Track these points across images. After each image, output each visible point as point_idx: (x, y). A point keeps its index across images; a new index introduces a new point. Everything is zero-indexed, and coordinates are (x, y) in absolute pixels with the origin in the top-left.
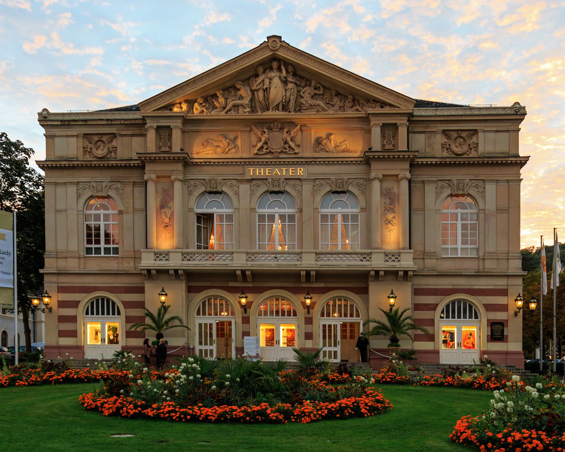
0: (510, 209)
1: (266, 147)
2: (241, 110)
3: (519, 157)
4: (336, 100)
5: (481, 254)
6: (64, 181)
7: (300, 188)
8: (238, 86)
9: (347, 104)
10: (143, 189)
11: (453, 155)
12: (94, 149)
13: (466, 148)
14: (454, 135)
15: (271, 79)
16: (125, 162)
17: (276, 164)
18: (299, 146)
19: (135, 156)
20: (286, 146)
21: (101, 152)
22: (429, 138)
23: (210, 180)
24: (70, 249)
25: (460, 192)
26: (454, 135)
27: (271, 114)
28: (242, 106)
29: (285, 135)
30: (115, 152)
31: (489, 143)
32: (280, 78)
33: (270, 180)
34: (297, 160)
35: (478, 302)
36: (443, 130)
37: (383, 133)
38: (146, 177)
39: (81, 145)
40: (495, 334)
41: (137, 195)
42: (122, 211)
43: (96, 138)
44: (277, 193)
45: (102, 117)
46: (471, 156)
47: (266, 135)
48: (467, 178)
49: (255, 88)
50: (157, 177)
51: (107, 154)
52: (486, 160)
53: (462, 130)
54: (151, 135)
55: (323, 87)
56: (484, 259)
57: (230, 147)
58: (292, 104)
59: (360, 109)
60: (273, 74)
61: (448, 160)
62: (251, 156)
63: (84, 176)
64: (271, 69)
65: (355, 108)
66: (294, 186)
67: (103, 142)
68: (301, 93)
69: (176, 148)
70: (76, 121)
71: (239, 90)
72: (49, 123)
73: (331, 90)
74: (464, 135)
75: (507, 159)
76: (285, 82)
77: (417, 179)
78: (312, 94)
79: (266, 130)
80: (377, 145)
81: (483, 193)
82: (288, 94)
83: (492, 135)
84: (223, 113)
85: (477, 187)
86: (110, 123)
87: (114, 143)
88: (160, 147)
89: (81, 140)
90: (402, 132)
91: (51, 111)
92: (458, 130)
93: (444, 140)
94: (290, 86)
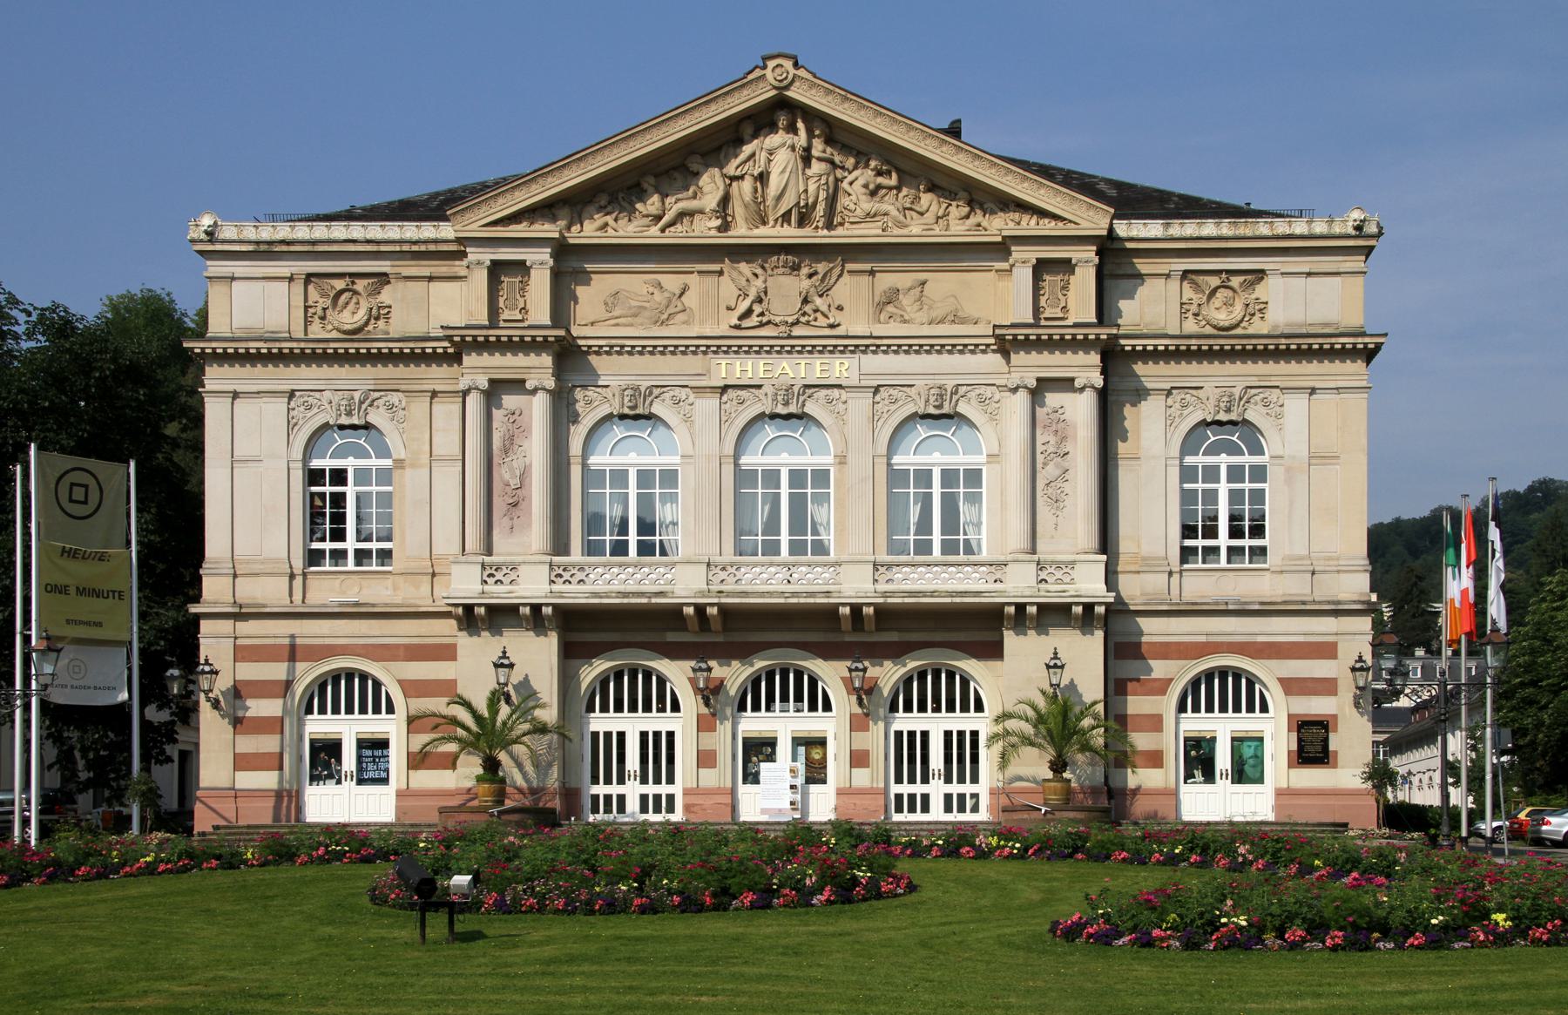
4: (926, 199)
8: (694, 167)
10: (457, 407)
16: (412, 345)
18: (840, 308)
20: (808, 308)
21: (350, 318)
28: (701, 212)
29: (806, 284)
30: (387, 317)
32: (793, 148)
34: (834, 342)
35: (1267, 672)
36: (1186, 272)
40: (1308, 748)
42: (402, 461)
46: (1250, 331)
47: (759, 283)
51: (367, 323)
52: (1283, 341)
55: (898, 171)
57: (671, 310)
61: (1193, 342)
62: (723, 329)
64: (772, 127)
65: (973, 220)
75: (1333, 340)
76: (807, 159)
78: (872, 186)
79: (759, 271)
82: (812, 188)
83: (1301, 280)
84: (655, 230)
87: (386, 296)
89: (298, 287)
93: (1188, 293)
94: (817, 167)
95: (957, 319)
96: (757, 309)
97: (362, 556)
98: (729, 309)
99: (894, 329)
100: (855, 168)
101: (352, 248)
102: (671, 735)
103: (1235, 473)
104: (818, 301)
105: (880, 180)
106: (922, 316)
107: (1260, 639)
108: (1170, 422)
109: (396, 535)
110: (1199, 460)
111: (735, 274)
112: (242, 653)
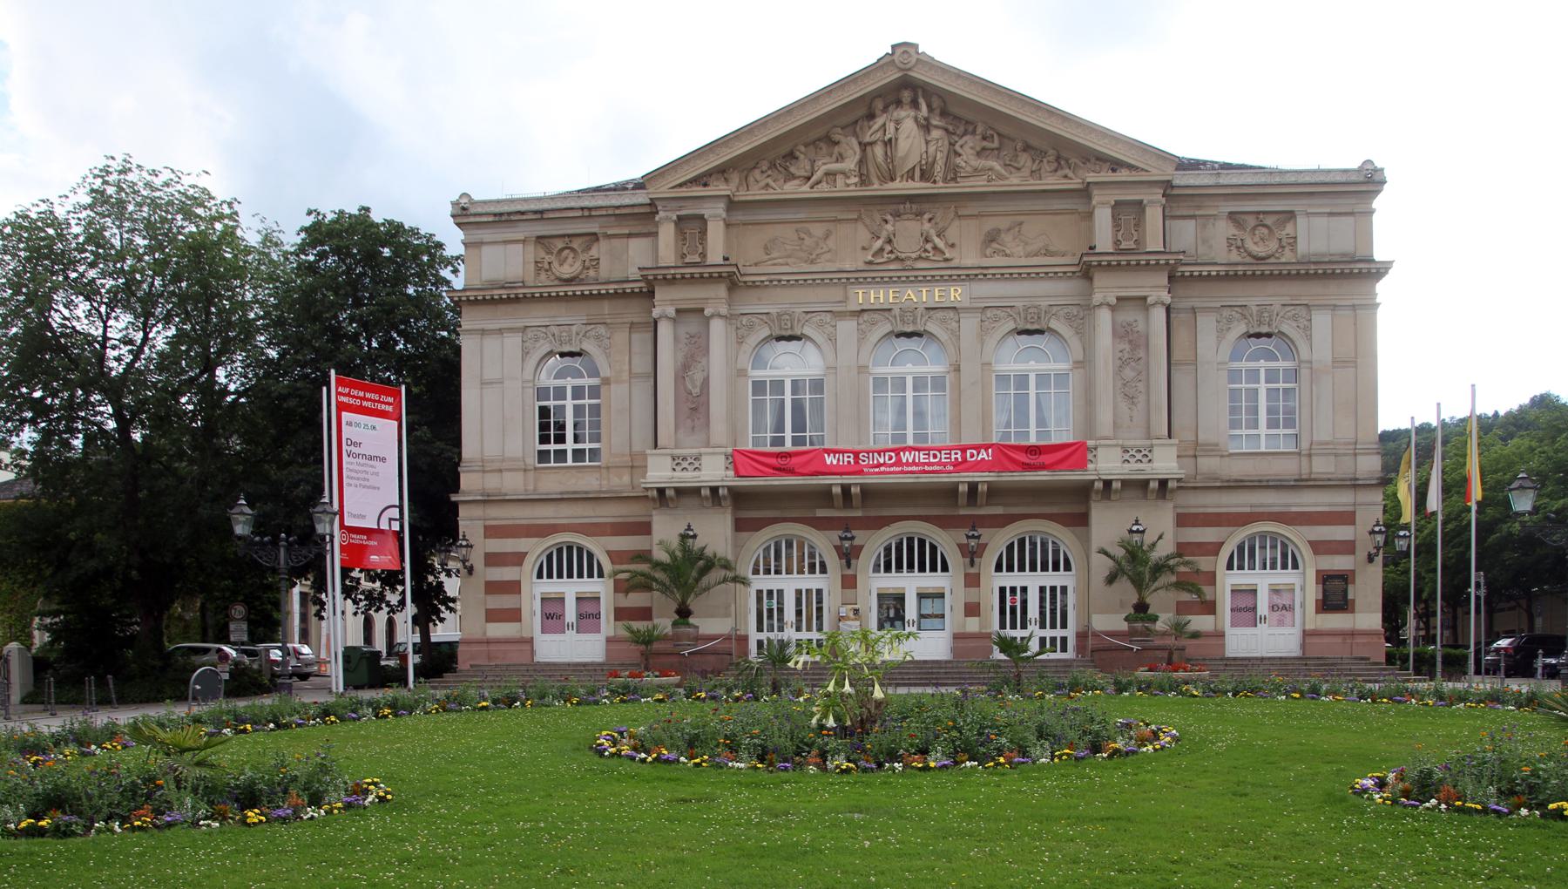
0: (1357, 362)
1: (888, 248)
2: (840, 180)
3: (1373, 261)
4: (1024, 159)
5: (1305, 445)
6: (498, 326)
7: (955, 325)
8: (836, 137)
9: (1046, 167)
10: (650, 335)
11: (1248, 260)
12: (555, 264)
13: (1273, 246)
14: (1251, 221)
15: (898, 122)
17: (908, 281)
18: (953, 246)
19: (633, 273)
20: (929, 246)
21: (567, 270)
22: (1204, 226)
23: (779, 315)
24: (507, 455)
25: (1265, 329)
26: (1251, 221)
27: (899, 187)
28: (843, 173)
29: (927, 226)
31: (1316, 236)
32: (916, 119)
33: (897, 312)
34: (949, 272)
37: (1115, 218)
38: (656, 313)
39: (531, 258)
41: (636, 348)
43: (560, 244)
44: (909, 335)
45: (573, 204)
47: (889, 227)
48: (1277, 302)
49: (867, 139)
50: (678, 311)
53: (1264, 213)
54: (667, 233)
56: (1310, 455)
58: (939, 168)
59: (1071, 174)
60: (902, 113)
63: (536, 316)
65: (1060, 173)
66: (943, 321)
67: (572, 250)
68: (957, 147)
69: (715, 255)
70: (522, 213)
71: (837, 143)
72: (472, 219)
73: (1013, 140)
74: (1269, 221)
76: (926, 127)
77: (1181, 305)
79: (889, 217)
80: (1104, 239)
81: (1307, 330)
82: (932, 149)
84: (806, 188)
85: (1295, 318)
86: (588, 213)
87: (594, 252)
88: (683, 256)
89: (531, 248)
90: (1154, 216)
91: (476, 197)
92: (1259, 213)
93: (1232, 231)
94: (936, 134)
95: (1048, 253)
96: (888, 248)
97: (579, 455)
98: (864, 248)
99: (998, 261)
100: (965, 133)
101: (571, 214)
102: (819, 592)
103: (1272, 376)
104: (937, 240)
105: (985, 144)
106: (1019, 250)
107: (1294, 509)
108: (1221, 333)
109: (604, 437)
110: (1244, 365)
111: (868, 221)
112: (492, 532)
